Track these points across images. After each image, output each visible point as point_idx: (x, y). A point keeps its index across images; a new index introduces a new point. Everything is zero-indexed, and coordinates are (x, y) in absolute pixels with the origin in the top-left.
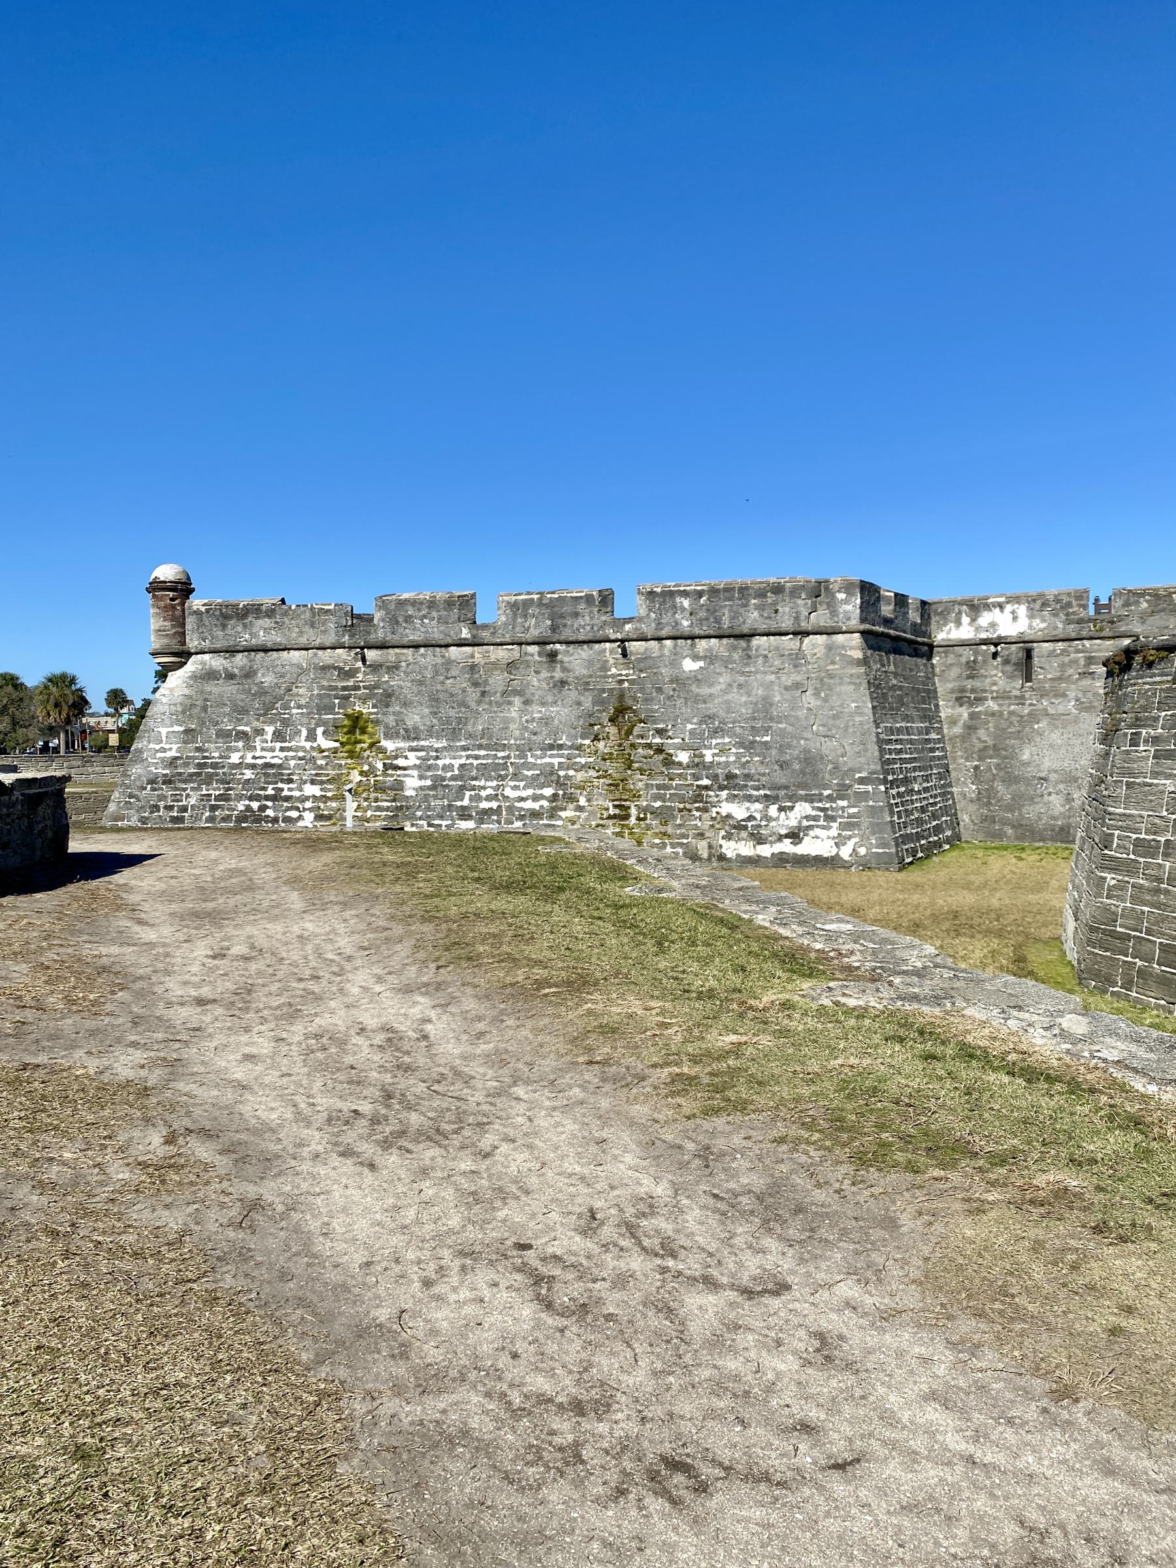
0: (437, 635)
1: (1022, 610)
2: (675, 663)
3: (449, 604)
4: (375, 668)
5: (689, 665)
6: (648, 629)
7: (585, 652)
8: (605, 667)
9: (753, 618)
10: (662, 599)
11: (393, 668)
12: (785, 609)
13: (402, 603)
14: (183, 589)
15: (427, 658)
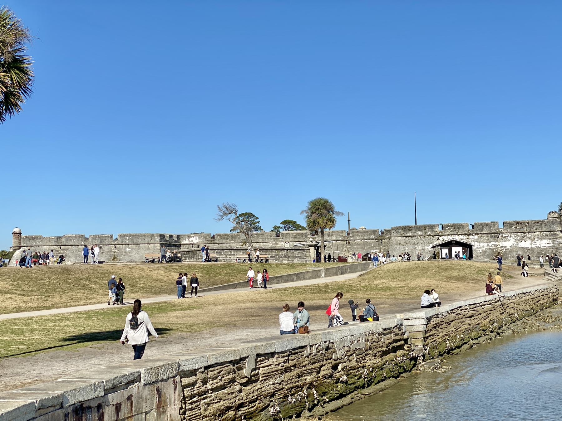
0: (77, 244)
1: (197, 238)
2: (125, 249)
3: (79, 237)
4: (63, 250)
5: (128, 250)
6: (120, 243)
7: (107, 247)
8: (111, 250)
9: (140, 241)
10: (123, 237)
11: (67, 250)
12: (146, 239)
13: (69, 237)
14: (20, 233)
15: (74, 248)
